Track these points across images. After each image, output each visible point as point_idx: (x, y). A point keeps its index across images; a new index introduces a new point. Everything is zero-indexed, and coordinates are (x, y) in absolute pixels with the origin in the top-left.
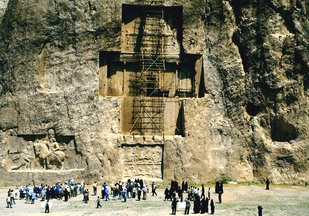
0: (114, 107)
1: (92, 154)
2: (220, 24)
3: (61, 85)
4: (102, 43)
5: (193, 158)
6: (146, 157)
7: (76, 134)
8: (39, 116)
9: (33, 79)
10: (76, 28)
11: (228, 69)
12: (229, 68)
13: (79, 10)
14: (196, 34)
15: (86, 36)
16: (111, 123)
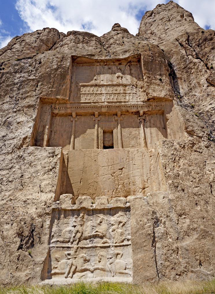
0: (49, 157)
2: (187, 76)
5: (191, 227)
6: (97, 233)
10: (16, 78)
11: (212, 109)
12: (212, 108)
14: (160, 80)
16: (42, 178)
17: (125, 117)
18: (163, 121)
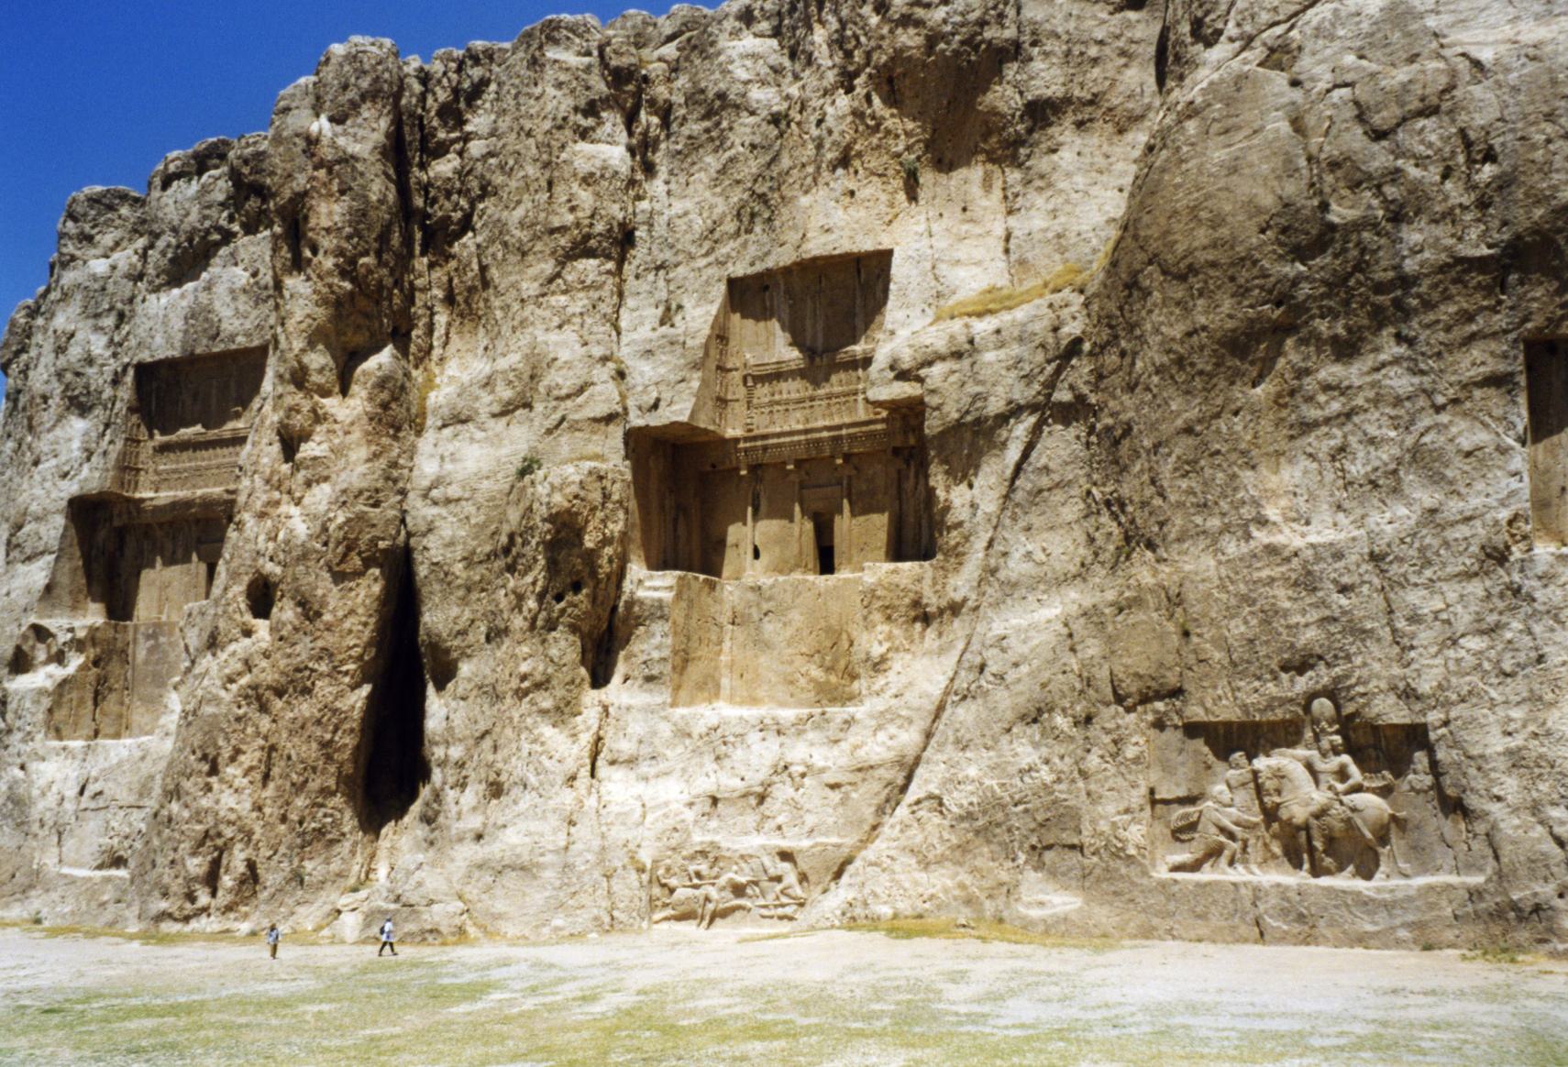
1: (1515, 810)
3: (1355, 503)
4: (1534, 299)
7: (1434, 717)
8: (1267, 642)
9: (1236, 489)
10: (1406, 253)
13: (1414, 172)
15: (1455, 281)
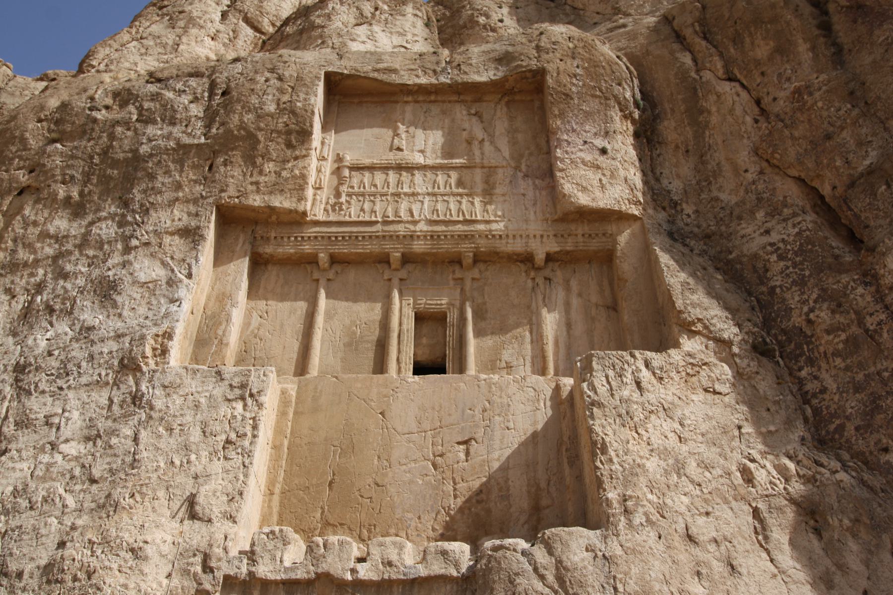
10: (144, 141)
11: (769, 248)
17: (487, 270)
18: (611, 284)
